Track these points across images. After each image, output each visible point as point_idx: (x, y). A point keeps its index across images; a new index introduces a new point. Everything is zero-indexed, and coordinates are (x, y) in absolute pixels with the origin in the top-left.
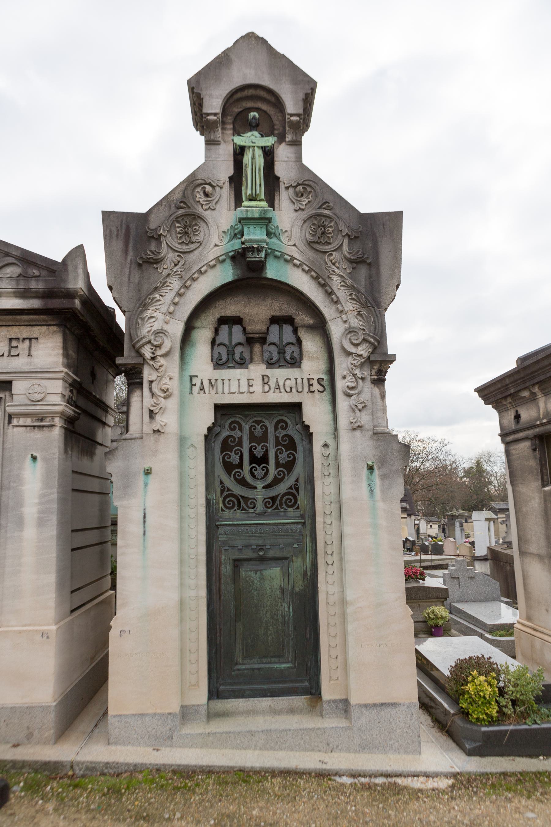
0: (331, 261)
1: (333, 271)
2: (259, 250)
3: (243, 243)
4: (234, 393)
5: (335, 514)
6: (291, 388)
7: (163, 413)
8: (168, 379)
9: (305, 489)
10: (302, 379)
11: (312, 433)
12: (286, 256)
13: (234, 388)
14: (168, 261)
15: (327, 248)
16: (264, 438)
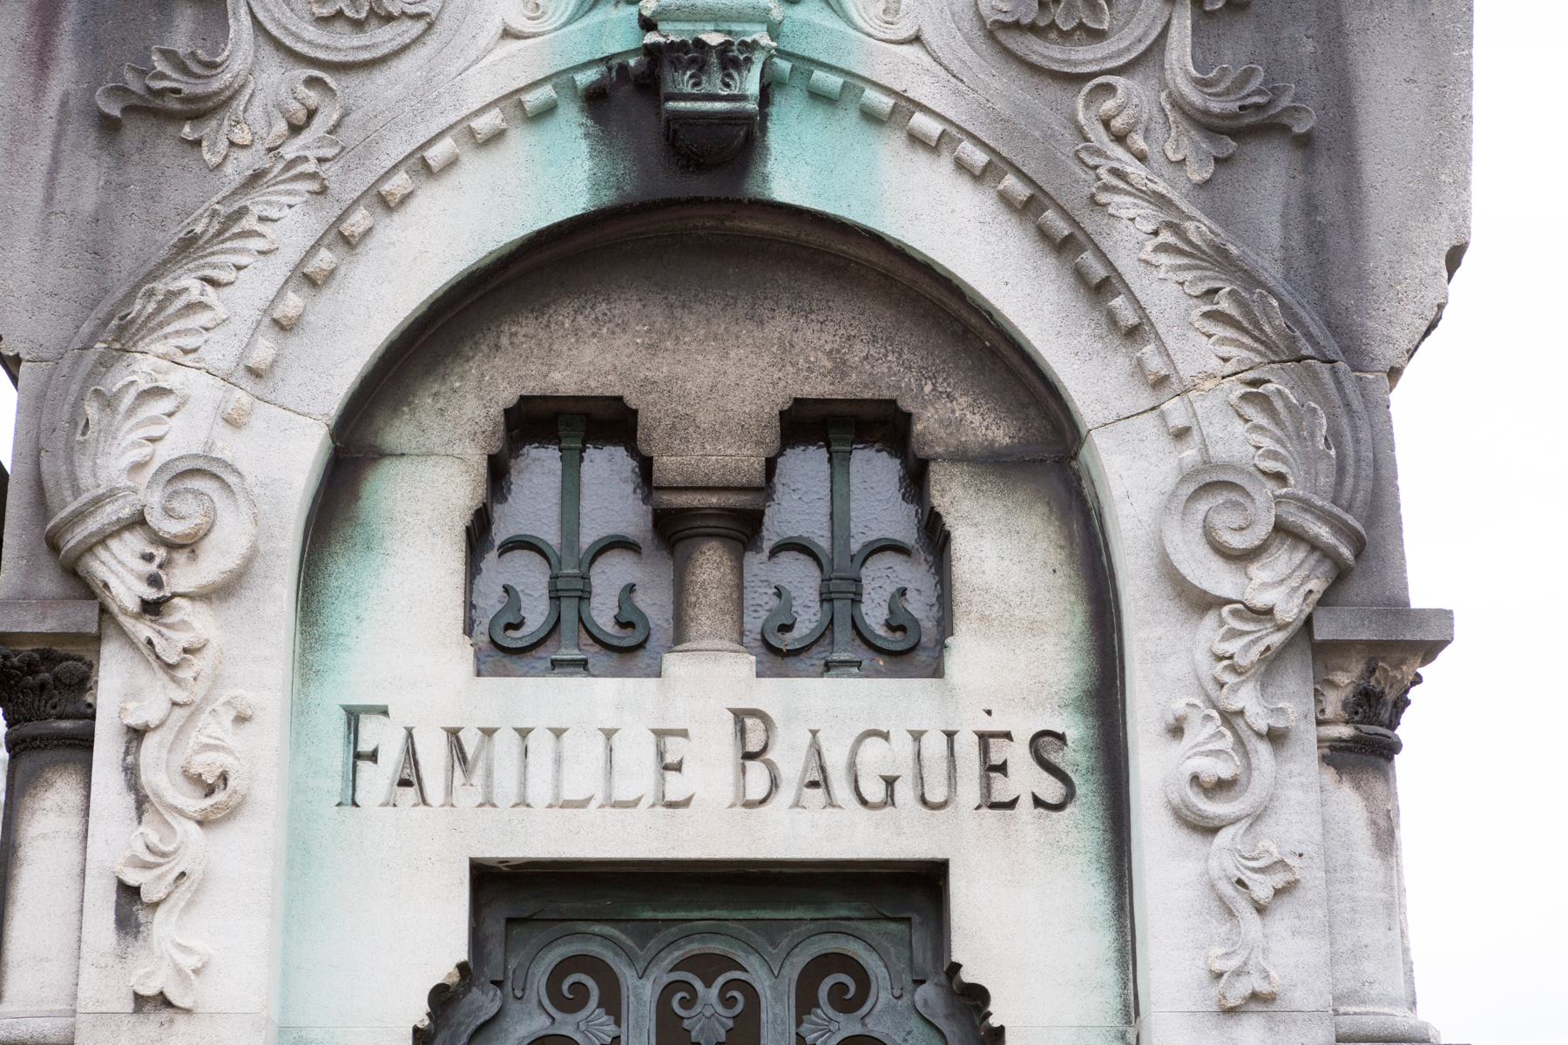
0: (1106, 124)
1: (1115, 172)
2: (731, 59)
3: (648, 24)
4: (583, 804)
6: (890, 782)
7: (190, 904)
8: (228, 717)
10: (950, 735)
11: (1002, 1028)
12: (872, 96)
13: (582, 779)
14: (256, 111)
15: (1085, 56)
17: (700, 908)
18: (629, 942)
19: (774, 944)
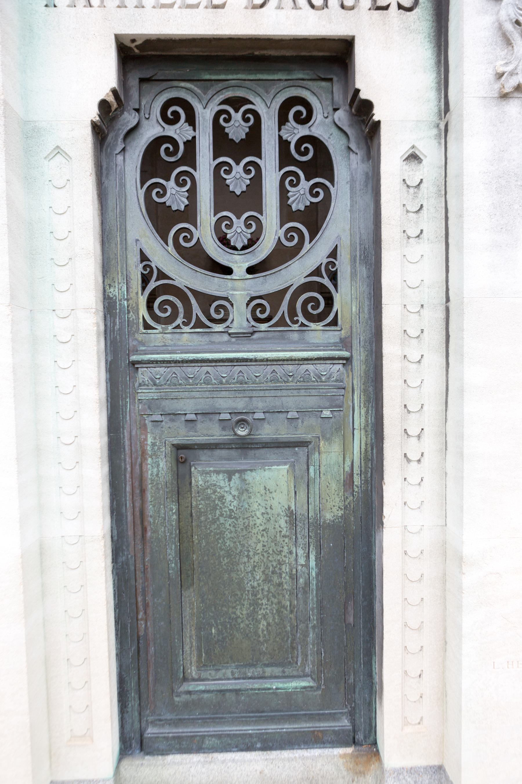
5: (434, 336)
9: (353, 275)
11: (379, 122)
16: (252, 143)
17: (232, 74)
18: (198, 91)
19: (267, 92)
